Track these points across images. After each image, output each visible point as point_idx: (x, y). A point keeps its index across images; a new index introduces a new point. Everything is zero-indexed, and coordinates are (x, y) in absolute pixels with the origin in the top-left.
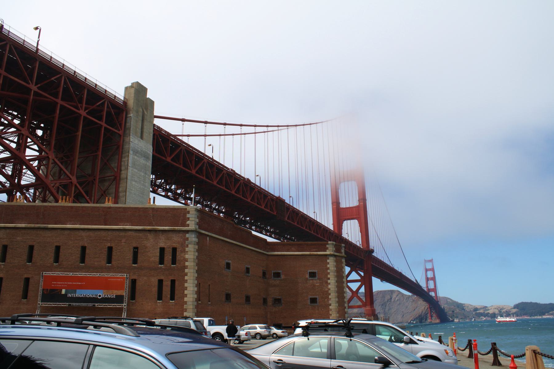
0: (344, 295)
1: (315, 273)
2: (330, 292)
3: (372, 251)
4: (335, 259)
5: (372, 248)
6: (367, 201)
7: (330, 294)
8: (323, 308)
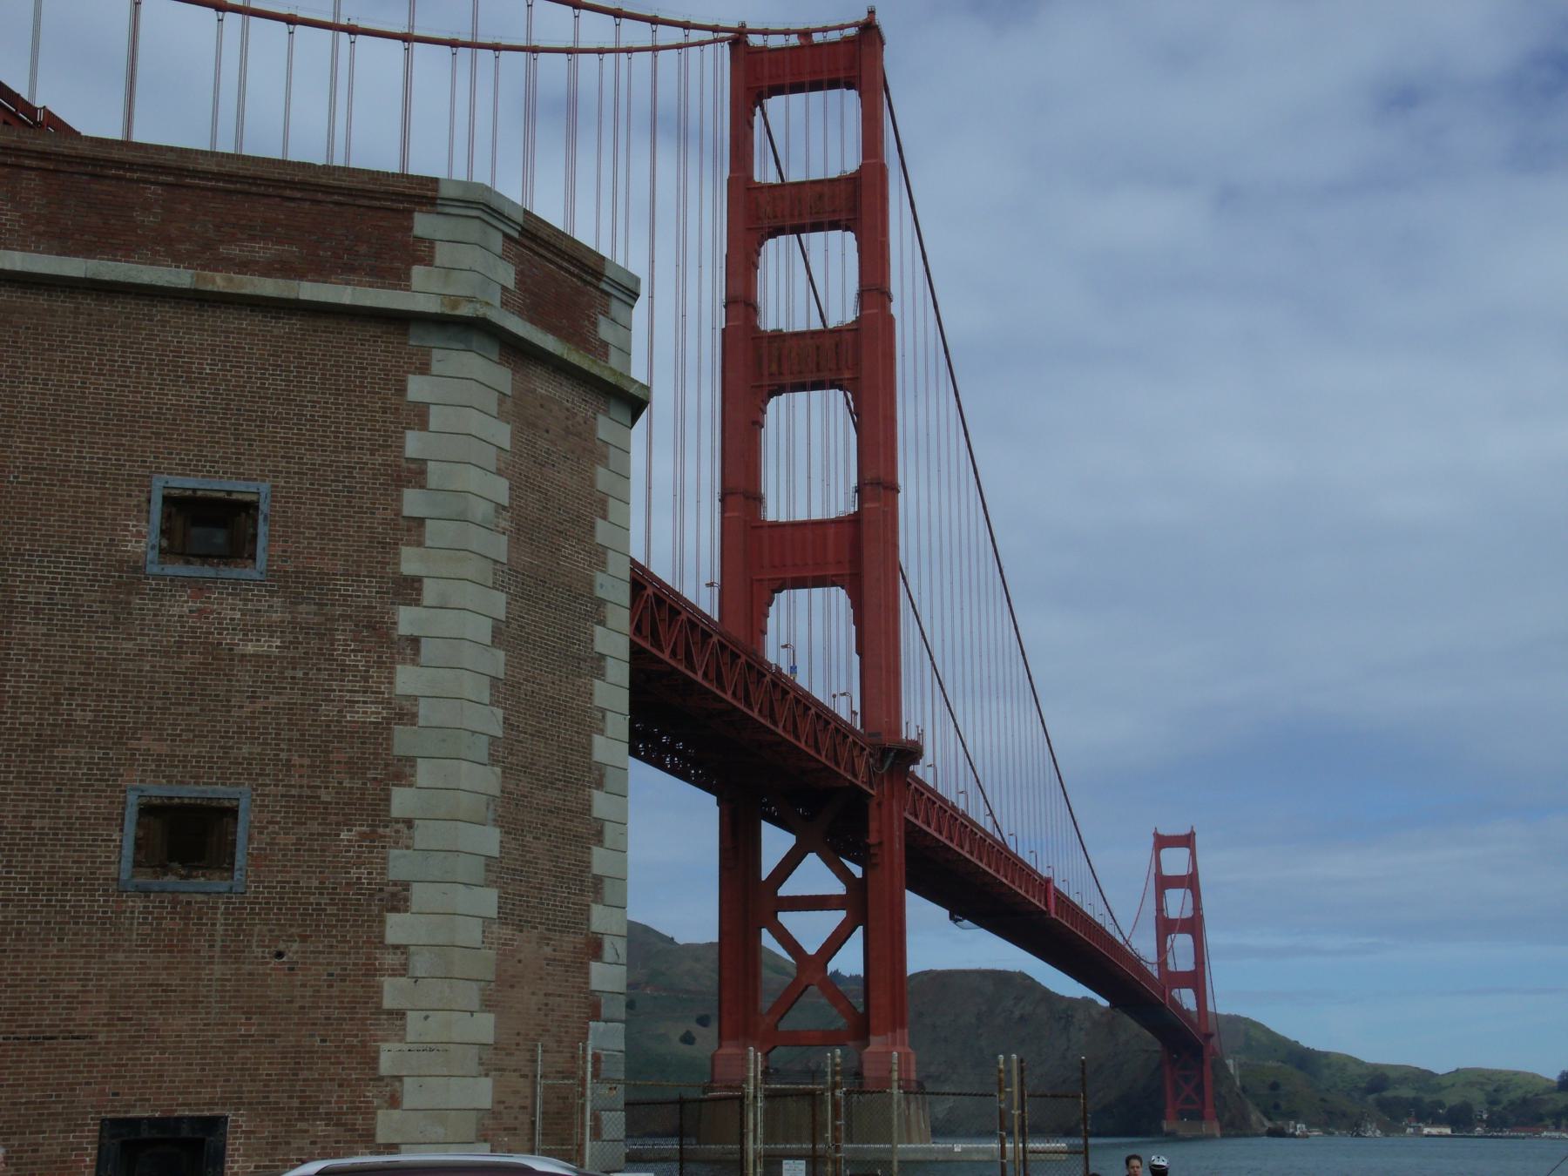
0: (587, 808)
1: (248, 508)
2: (403, 740)
3: (912, 753)
4: (502, 377)
5: (913, 736)
6: (901, 496)
7: (401, 772)
8: (304, 938)
